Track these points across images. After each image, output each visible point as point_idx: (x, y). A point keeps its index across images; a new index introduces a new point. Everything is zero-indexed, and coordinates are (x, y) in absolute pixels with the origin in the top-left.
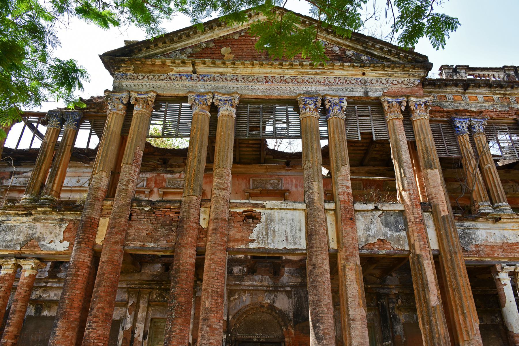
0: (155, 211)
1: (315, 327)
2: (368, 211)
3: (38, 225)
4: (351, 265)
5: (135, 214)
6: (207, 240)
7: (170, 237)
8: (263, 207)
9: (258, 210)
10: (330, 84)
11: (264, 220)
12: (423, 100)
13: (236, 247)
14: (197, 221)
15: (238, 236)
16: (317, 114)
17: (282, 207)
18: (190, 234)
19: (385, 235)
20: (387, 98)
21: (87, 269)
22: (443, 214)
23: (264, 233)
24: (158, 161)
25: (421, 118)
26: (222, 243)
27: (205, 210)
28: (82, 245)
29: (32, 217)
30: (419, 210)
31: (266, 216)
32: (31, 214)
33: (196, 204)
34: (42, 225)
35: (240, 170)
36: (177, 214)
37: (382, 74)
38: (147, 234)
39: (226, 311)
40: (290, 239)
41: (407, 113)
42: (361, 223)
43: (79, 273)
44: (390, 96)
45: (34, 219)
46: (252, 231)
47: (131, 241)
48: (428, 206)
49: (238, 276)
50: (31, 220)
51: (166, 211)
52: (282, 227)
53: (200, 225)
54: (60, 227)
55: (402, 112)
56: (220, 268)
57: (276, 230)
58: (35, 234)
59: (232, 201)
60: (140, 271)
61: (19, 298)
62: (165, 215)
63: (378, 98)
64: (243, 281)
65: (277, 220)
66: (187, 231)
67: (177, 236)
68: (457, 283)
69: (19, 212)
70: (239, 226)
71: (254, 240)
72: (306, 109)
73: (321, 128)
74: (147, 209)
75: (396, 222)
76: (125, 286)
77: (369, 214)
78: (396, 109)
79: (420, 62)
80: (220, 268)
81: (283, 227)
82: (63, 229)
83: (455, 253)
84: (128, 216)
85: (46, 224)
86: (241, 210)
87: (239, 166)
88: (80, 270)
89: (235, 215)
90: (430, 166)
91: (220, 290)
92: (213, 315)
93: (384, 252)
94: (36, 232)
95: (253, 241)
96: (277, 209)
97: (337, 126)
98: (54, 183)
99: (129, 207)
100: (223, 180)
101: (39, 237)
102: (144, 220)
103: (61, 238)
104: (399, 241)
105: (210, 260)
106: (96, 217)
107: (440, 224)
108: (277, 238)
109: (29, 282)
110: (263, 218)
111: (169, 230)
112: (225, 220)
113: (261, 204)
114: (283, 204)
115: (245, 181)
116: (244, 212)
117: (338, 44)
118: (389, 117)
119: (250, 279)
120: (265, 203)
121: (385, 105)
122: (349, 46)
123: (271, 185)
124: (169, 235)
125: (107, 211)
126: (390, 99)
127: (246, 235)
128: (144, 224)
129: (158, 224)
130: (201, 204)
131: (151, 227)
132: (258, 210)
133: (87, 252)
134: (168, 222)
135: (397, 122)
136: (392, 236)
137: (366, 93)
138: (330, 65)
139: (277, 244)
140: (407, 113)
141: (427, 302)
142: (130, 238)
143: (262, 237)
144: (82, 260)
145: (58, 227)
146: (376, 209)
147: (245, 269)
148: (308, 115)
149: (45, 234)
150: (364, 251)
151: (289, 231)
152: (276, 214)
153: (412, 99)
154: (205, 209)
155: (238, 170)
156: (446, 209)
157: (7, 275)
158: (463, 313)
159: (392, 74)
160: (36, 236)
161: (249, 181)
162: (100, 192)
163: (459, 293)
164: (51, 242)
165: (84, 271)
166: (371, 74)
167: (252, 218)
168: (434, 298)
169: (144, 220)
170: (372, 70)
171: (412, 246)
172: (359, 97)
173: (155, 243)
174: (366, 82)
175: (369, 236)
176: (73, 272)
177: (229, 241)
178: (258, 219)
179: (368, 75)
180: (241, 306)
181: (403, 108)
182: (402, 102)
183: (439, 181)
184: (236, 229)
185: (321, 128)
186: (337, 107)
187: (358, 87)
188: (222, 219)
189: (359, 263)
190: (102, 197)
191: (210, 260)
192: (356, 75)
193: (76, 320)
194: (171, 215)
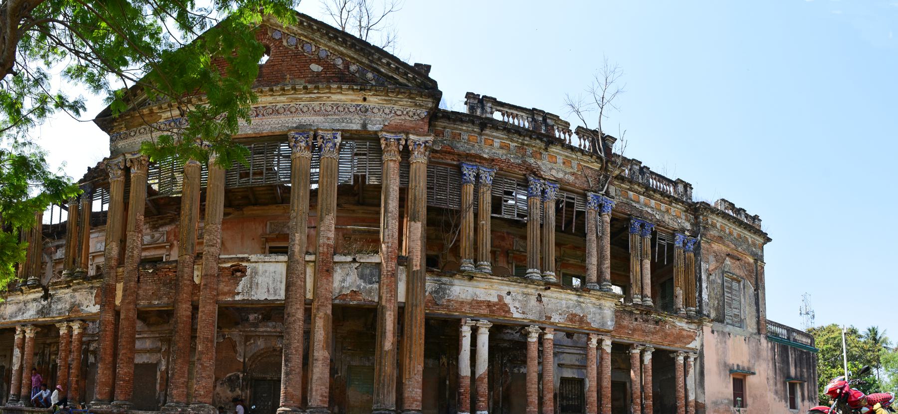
1: (286, 365)
2: (346, 262)
4: (321, 314)
8: (248, 260)
9: (244, 264)
10: (326, 114)
12: (423, 139)
15: (226, 289)
16: (307, 154)
19: (358, 286)
20: (384, 133)
22: (415, 269)
25: (419, 160)
30: (393, 264)
37: (385, 100)
40: (272, 291)
41: (406, 153)
42: (338, 275)
44: (388, 132)
48: (403, 261)
52: (267, 278)
55: (400, 152)
63: (376, 132)
65: (260, 272)
68: (411, 333)
72: (297, 147)
73: (313, 170)
75: (372, 275)
77: (347, 266)
78: (393, 148)
79: (428, 89)
83: (416, 306)
86: (229, 265)
90: (414, 219)
93: (355, 302)
95: (238, 293)
97: (327, 167)
100: (212, 237)
104: (370, 292)
105: (202, 312)
107: (412, 279)
108: (260, 290)
110: (249, 271)
112: (214, 276)
117: (342, 54)
118: (385, 157)
121: (382, 141)
122: (353, 58)
126: (388, 135)
132: (244, 264)
135: (392, 164)
136: (365, 287)
137: (364, 126)
138: (327, 88)
139: (260, 295)
140: (406, 153)
141: (382, 347)
146: (354, 260)
148: (298, 155)
150: (337, 302)
151: (270, 283)
152: (261, 267)
153: (411, 137)
156: (418, 264)
158: (410, 357)
159: (396, 102)
163: (411, 341)
166: (374, 100)
167: (237, 271)
168: (389, 343)
170: (374, 95)
171: (380, 298)
172: (356, 131)
174: (367, 110)
175: (343, 287)
177: (218, 295)
179: (370, 101)
181: (401, 147)
182: (400, 139)
183: (419, 235)
185: (313, 170)
186: (330, 145)
187: (357, 116)
188: (211, 275)
189: (329, 312)
191: (202, 312)
192: (355, 100)
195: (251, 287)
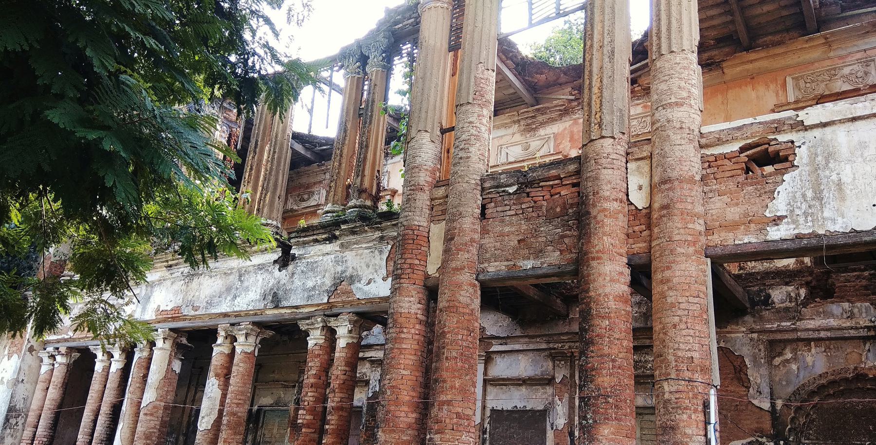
0: (528, 190)
3: (349, 255)
5: (493, 204)
6: (651, 236)
7: (566, 240)
9: (782, 138)
11: (805, 160)
13: (730, 242)
14: (622, 195)
15: (733, 213)
17: (858, 114)
18: (607, 229)
21: (418, 326)
23: (810, 194)
24: (571, 94)
26: (690, 238)
27: (638, 167)
28: (402, 281)
29: (339, 242)
31: (809, 147)
32: (335, 238)
33: (614, 156)
34: (354, 253)
35: (757, 64)
36: (574, 189)
38: (519, 241)
39: (766, 390)
43: (403, 336)
45: (342, 246)
46: (771, 195)
47: (488, 261)
49: (787, 309)
50: (338, 248)
51: (552, 186)
53: (632, 204)
54: (381, 252)
56: (691, 299)
57: (844, 179)
58: (345, 271)
59: (705, 130)
60: (568, 315)
61: (337, 386)
62: (552, 196)
64: (801, 320)
66: (598, 223)
67: (579, 238)
69: (319, 237)
70: (732, 185)
71: (781, 218)
74: (511, 190)
76: (544, 346)
80: (691, 299)
81: (868, 168)
82: (385, 257)
84: (479, 211)
85: (360, 252)
86: (735, 147)
87: (752, 56)
88: (405, 330)
89: (719, 163)
91: (696, 355)
92: (685, 417)
94: (347, 267)
95: (777, 220)
96: (841, 121)
98: (363, 176)
99: (479, 193)
101: (351, 277)
102: (509, 213)
103: (384, 272)
106: (422, 224)
109: (349, 355)
111: (563, 226)
112: (691, 181)
113: (790, 118)
114: (860, 105)
115: (772, 87)
116: (743, 150)
119: (819, 314)
120: (801, 113)
123: (846, 78)
124: (562, 237)
125: (441, 208)
127: (755, 209)
128: (511, 224)
129: (539, 216)
130: (628, 154)
131: (524, 227)
132: (782, 138)
133: (414, 293)
134: (558, 210)
142: (488, 255)
143: (804, 206)
144: (406, 311)
145: (377, 252)
147: (803, 292)
149: (359, 269)
152: (841, 136)
154: (639, 163)
155: (750, 66)
157: (317, 348)
160: (348, 274)
161: (784, 85)
162: (422, 174)
164: (369, 283)
165: (413, 331)
169: (509, 213)
173: (536, 257)
176: (394, 335)
178: (785, 159)
180: (804, 377)
184: (725, 198)
190: (427, 182)
193: (409, 426)
194: (563, 193)
195: (819, 197)
